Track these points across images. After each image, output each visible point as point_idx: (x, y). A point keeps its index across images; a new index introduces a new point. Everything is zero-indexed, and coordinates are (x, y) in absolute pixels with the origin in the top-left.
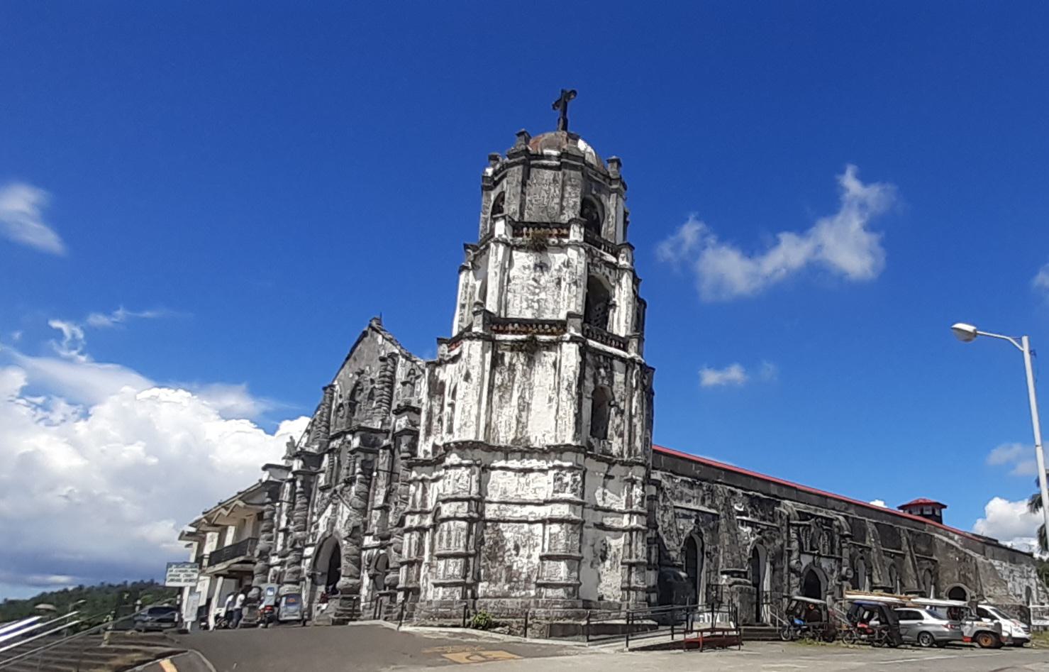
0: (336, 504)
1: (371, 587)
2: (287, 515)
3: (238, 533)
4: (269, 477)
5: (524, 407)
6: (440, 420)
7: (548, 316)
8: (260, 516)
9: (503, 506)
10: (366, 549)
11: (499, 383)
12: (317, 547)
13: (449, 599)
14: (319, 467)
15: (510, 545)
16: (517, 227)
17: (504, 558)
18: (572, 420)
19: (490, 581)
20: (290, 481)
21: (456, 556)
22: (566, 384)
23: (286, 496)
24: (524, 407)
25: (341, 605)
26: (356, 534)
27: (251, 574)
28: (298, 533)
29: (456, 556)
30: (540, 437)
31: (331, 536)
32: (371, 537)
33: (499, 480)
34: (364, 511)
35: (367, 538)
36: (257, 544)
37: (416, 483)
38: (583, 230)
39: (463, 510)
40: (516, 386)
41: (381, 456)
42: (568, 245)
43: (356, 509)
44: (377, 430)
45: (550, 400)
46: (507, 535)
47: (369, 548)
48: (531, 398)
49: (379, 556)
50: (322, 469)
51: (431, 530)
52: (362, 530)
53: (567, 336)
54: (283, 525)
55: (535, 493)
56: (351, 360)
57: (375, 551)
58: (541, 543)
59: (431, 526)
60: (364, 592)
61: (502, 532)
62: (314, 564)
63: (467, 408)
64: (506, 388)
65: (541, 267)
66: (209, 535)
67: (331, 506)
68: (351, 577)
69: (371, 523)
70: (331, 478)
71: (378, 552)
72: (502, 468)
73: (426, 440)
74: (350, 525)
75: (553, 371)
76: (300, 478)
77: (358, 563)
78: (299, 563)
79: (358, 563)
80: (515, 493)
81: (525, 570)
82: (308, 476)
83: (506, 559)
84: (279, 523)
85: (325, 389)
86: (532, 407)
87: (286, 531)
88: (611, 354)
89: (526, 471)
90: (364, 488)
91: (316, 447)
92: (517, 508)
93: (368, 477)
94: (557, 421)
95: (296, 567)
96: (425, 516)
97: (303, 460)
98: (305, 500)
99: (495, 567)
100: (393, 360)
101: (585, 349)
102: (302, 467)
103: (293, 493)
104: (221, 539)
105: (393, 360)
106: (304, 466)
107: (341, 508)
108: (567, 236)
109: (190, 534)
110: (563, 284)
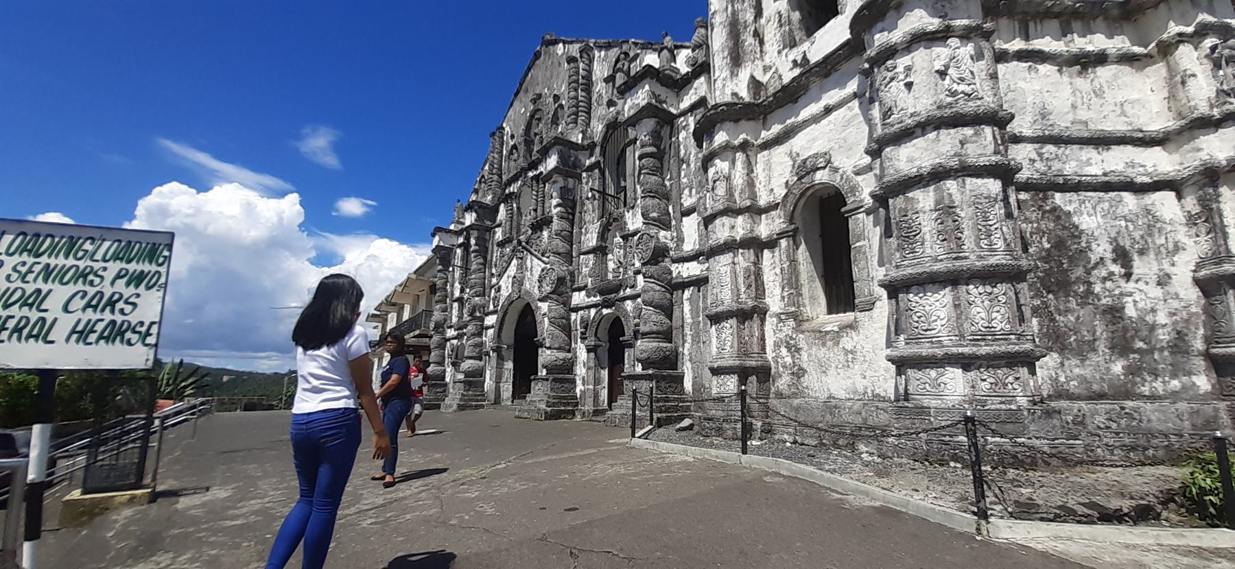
0: (521, 258)
1: (592, 364)
2: (460, 283)
3: (413, 310)
4: (439, 242)
6: (757, 35)
8: (433, 289)
9: (1050, 149)
10: (576, 310)
12: (501, 315)
14: (494, 222)
15: (1102, 249)
17: (1090, 284)
19: (1063, 349)
20: (460, 246)
21: (989, 276)
23: (458, 261)
25: (552, 389)
26: (563, 289)
27: (428, 349)
28: (477, 299)
29: (989, 276)
31: (519, 297)
32: (583, 293)
33: (1022, 84)
34: (568, 257)
35: (576, 294)
36: (431, 316)
37: (730, 154)
41: (584, 181)
43: (559, 254)
47: (582, 308)
50: (498, 222)
51: (784, 243)
52: (569, 284)
55: (1123, 114)
56: (521, 94)
57: (593, 311)
59: (782, 235)
60: (580, 370)
61: (1069, 214)
62: (499, 335)
66: (390, 316)
67: (514, 262)
68: (559, 349)
69: (580, 273)
70: (511, 229)
72: (1022, 56)
73: (733, 74)
74: (554, 277)
76: (474, 234)
77: (567, 329)
78: (480, 334)
80: (1071, 117)
82: (484, 229)
83: (1097, 288)
84: (452, 294)
85: (493, 134)
87: (460, 300)
89: (1087, 62)
90: (566, 225)
91: (489, 198)
92: (1089, 153)
93: (570, 211)
95: (477, 339)
96: (756, 218)
97: (476, 212)
98: (481, 261)
99: (1068, 311)
100: (589, 55)
102: (476, 220)
103: (466, 258)
104: (399, 316)
105: (589, 55)
106: (479, 218)
109: (374, 316)
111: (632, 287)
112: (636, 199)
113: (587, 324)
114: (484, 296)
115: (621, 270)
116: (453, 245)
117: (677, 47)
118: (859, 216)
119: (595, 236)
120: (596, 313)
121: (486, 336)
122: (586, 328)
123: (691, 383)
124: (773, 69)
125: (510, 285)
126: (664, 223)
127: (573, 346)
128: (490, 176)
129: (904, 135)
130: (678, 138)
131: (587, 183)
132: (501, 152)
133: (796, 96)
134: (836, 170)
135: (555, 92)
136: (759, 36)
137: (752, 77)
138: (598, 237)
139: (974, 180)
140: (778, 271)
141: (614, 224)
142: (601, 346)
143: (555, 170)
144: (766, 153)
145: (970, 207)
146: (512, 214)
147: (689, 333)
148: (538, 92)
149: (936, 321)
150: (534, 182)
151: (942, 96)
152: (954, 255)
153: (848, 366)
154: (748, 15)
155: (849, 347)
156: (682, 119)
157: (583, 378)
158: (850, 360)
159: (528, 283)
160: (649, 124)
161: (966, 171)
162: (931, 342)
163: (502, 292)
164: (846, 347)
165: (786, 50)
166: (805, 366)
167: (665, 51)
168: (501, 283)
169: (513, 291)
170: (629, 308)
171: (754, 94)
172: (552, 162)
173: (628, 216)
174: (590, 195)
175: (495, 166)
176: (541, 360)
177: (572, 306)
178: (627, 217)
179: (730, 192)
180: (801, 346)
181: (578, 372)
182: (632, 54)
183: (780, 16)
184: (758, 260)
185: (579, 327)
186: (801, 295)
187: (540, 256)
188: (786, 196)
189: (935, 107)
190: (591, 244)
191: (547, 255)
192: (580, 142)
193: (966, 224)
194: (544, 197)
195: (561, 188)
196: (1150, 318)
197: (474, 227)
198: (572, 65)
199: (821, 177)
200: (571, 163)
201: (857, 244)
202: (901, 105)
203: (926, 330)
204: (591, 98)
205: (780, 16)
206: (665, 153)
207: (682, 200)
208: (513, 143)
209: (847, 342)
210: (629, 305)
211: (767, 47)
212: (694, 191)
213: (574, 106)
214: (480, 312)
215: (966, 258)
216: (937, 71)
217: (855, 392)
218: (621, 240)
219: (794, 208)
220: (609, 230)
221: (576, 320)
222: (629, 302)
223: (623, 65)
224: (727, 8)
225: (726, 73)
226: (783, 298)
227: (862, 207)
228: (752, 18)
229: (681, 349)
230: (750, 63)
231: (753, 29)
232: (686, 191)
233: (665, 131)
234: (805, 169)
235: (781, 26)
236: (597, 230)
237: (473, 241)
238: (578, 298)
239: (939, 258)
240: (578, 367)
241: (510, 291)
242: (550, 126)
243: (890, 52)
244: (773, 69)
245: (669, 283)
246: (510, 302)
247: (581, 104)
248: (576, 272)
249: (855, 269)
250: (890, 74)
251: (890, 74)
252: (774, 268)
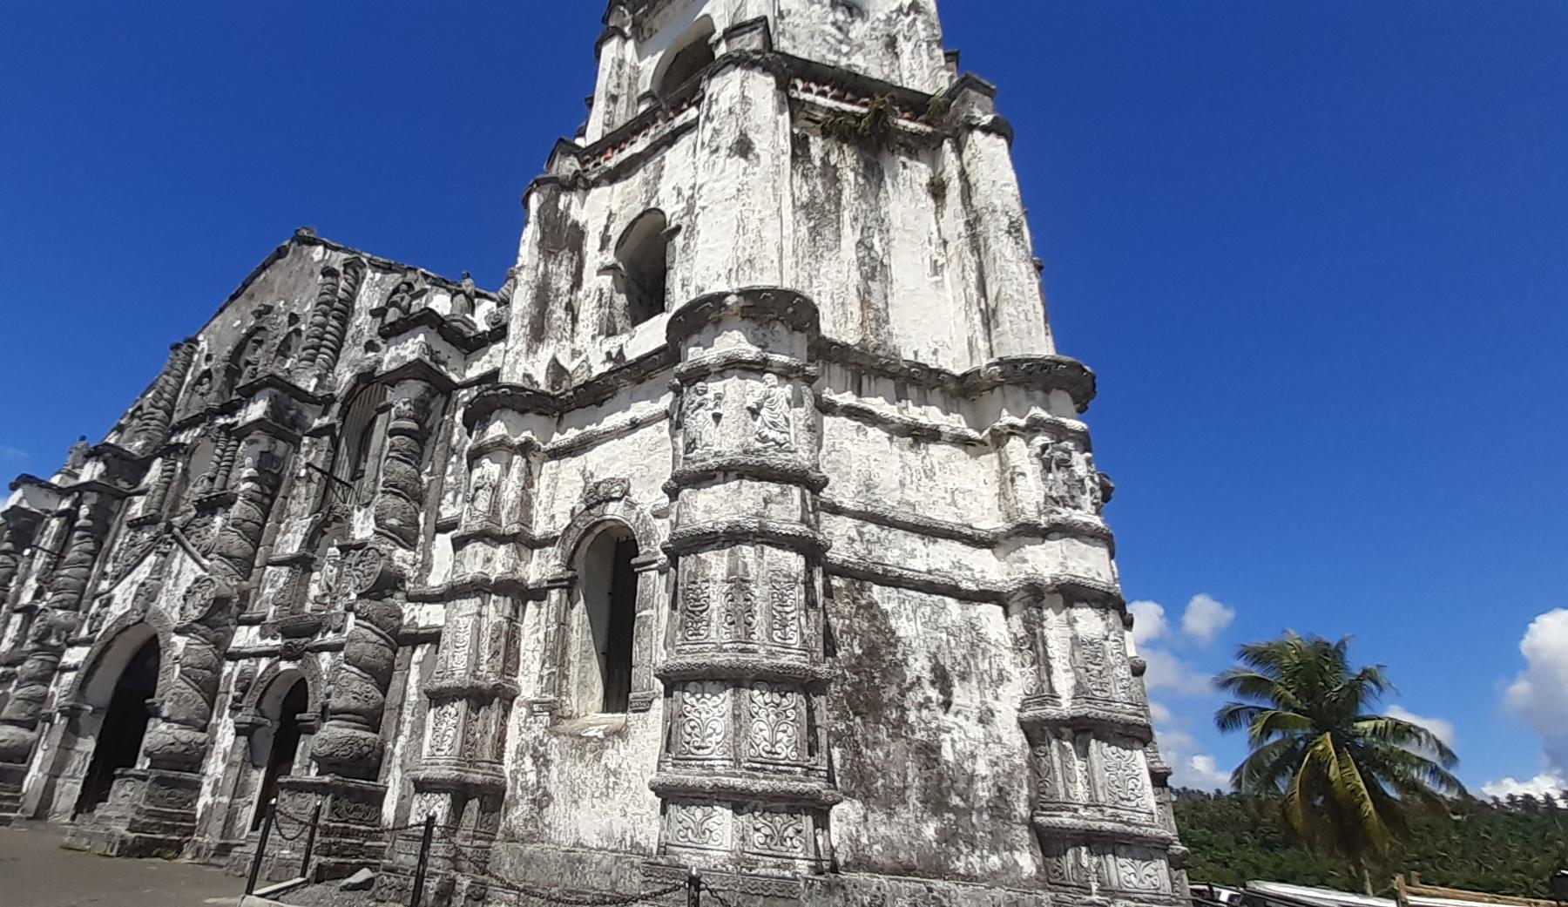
0: (165, 555)
1: (238, 757)
4: (21, 500)
5: (874, 269)
6: (570, 308)
10: (235, 657)
12: (97, 648)
13: (766, 868)
21: (778, 681)
24: (874, 269)
25: (149, 798)
26: (218, 617)
28: (60, 612)
29: (778, 681)
31: (141, 621)
32: (256, 629)
34: (245, 566)
35: (244, 629)
39: (787, 510)
41: (303, 449)
47: (247, 656)
49: (274, 677)
50: (142, 486)
51: (555, 595)
52: (234, 610)
57: (264, 663)
59: (554, 583)
60: (215, 767)
63: (753, 223)
67: (152, 558)
68: (185, 723)
69: (258, 595)
70: (162, 502)
73: (531, 350)
74: (210, 594)
76: (92, 498)
77: (210, 689)
78: (45, 680)
79: (210, 689)
82: (110, 497)
85: (176, 347)
86: (896, 271)
90: (255, 512)
91: (138, 444)
93: (268, 491)
95: (40, 689)
96: (525, 553)
97: (105, 462)
98: (90, 546)
102: (101, 476)
105: (356, 272)
111: (338, 631)
112: (374, 493)
113: (249, 684)
114: (77, 609)
115: (328, 600)
116: (48, 511)
117: (478, 295)
118: (653, 574)
119: (300, 538)
120: (269, 667)
121: (56, 685)
122: (244, 690)
123: (394, 807)
124: (583, 357)
126: (406, 537)
127: (213, 721)
128: (152, 410)
129: (703, 478)
130: (453, 417)
131: (308, 453)
132: (183, 376)
133: (602, 397)
134: (632, 506)
135: (295, 310)
136: (573, 311)
137: (555, 360)
138: (303, 541)
139: (775, 551)
140: (541, 635)
141: (334, 525)
142: (260, 726)
143: (258, 423)
144: (554, 463)
145: (766, 584)
146: (170, 477)
147: (409, 718)
148: (268, 303)
149: (710, 735)
150: (223, 434)
151: (751, 439)
152: (741, 646)
153: (607, 796)
154: (563, 282)
155: (612, 766)
156: (465, 391)
157: (217, 781)
158: (611, 785)
159: (164, 598)
160: (414, 388)
161: (765, 537)
162: (702, 766)
163: (112, 608)
164: (609, 765)
165: (602, 337)
166: (552, 789)
167: (461, 297)
168: (117, 591)
169: (133, 609)
170: (324, 666)
171: (553, 382)
172: (256, 410)
173: (358, 516)
174: (303, 473)
175: (166, 396)
176: (147, 741)
177: (230, 649)
178: (355, 518)
179: (494, 508)
180: (552, 757)
182: (417, 288)
183: (602, 294)
184: (517, 616)
185: (232, 688)
186: (566, 677)
187: (198, 555)
188: (568, 528)
189: (740, 450)
190: (289, 551)
191: (210, 556)
192: (311, 390)
193: (759, 606)
194: (233, 461)
195: (262, 453)
197: (94, 487)
198: (329, 279)
199: (614, 510)
200: (287, 418)
201: (644, 613)
202: (706, 439)
203: (698, 748)
204: (345, 331)
205: (602, 294)
206: (430, 434)
207: (441, 508)
208: (206, 368)
209: (611, 758)
210: (325, 660)
211: (580, 327)
212: (460, 497)
213: (316, 337)
214: (58, 639)
215: (754, 651)
216: (749, 408)
217: (610, 838)
218: (338, 553)
219: (577, 547)
220: (325, 533)
221: (230, 674)
222: (326, 655)
223: (402, 299)
224: (538, 266)
225: (522, 346)
226: (541, 677)
227: (655, 562)
228: (568, 287)
229: (390, 746)
230: (555, 341)
231: (566, 300)
232: (450, 496)
233: (437, 403)
234: (596, 497)
235: (600, 306)
236: (305, 530)
237: (84, 511)
238: (245, 637)
239: (725, 646)
240: (212, 760)
241: (129, 607)
242: (272, 356)
243: (701, 373)
244: (583, 357)
245: (395, 633)
246: (122, 627)
247: (327, 336)
248: (253, 592)
249: (636, 648)
250: (698, 399)
251: (698, 399)
252: (538, 630)
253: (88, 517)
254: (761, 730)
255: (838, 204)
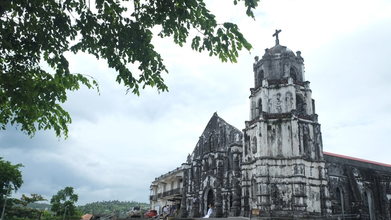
6: (250, 149)
7: (284, 111)
10: (223, 192)
11: (270, 136)
16: (270, 83)
18: (298, 147)
21: (264, 195)
22: (294, 135)
29: (264, 195)
30: (286, 154)
35: (223, 188)
38: (293, 80)
39: (265, 180)
40: (276, 137)
41: (224, 160)
42: (288, 86)
44: (222, 152)
45: (289, 141)
46: (280, 188)
47: (224, 192)
48: (282, 140)
53: (293, 118)
54: (190, 183)
58: (292, 191)
64: (272, 138)
65: (279, 95)
67: (207, 178)
69: (223, 184)
71: (227, 193)
73: (246, 156)
75: (289, 130)
81: (287, 201)
83: (280, 197)
84: (188, 184)
88: (307, 122)
94: (292, 148)
97: (196, 162)
101: (299, 122)
107: (211, 178)
108: (287, 83)
110: (288, 100)
122: (225, 197)
125: (206, 184)
131: (225, 161)
168: (204, 182)
181: (223, 207)
196: (285, 201)
253: (196, 171)
254: (263, 200)
255: (275, 135)
